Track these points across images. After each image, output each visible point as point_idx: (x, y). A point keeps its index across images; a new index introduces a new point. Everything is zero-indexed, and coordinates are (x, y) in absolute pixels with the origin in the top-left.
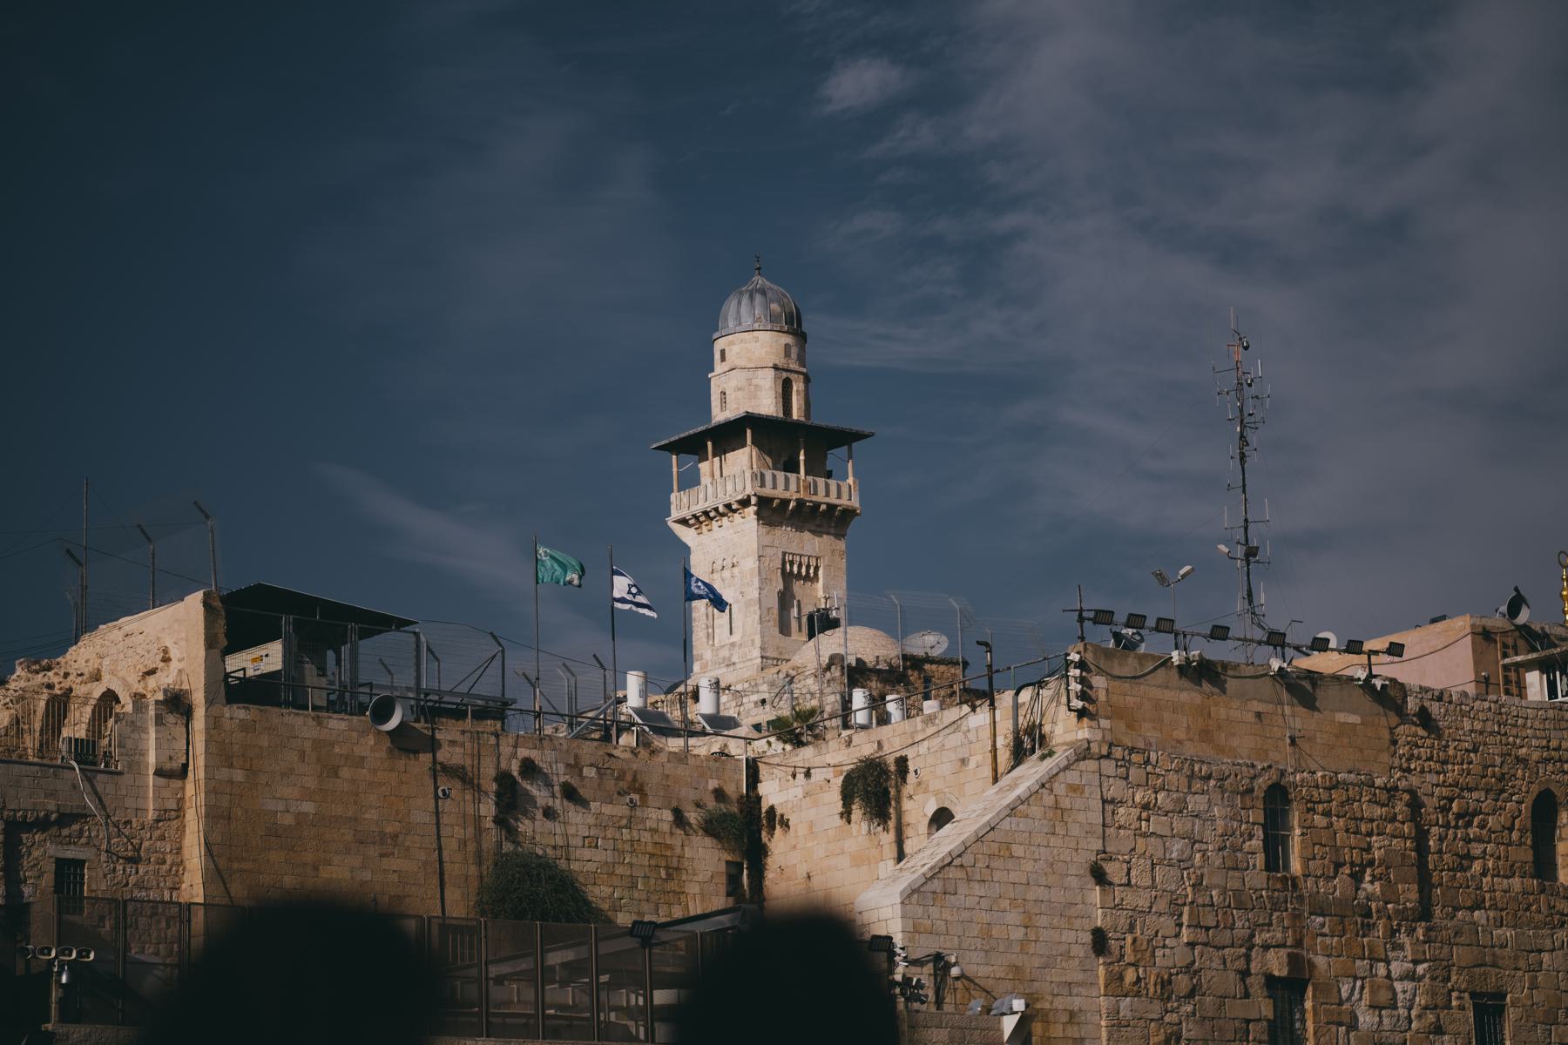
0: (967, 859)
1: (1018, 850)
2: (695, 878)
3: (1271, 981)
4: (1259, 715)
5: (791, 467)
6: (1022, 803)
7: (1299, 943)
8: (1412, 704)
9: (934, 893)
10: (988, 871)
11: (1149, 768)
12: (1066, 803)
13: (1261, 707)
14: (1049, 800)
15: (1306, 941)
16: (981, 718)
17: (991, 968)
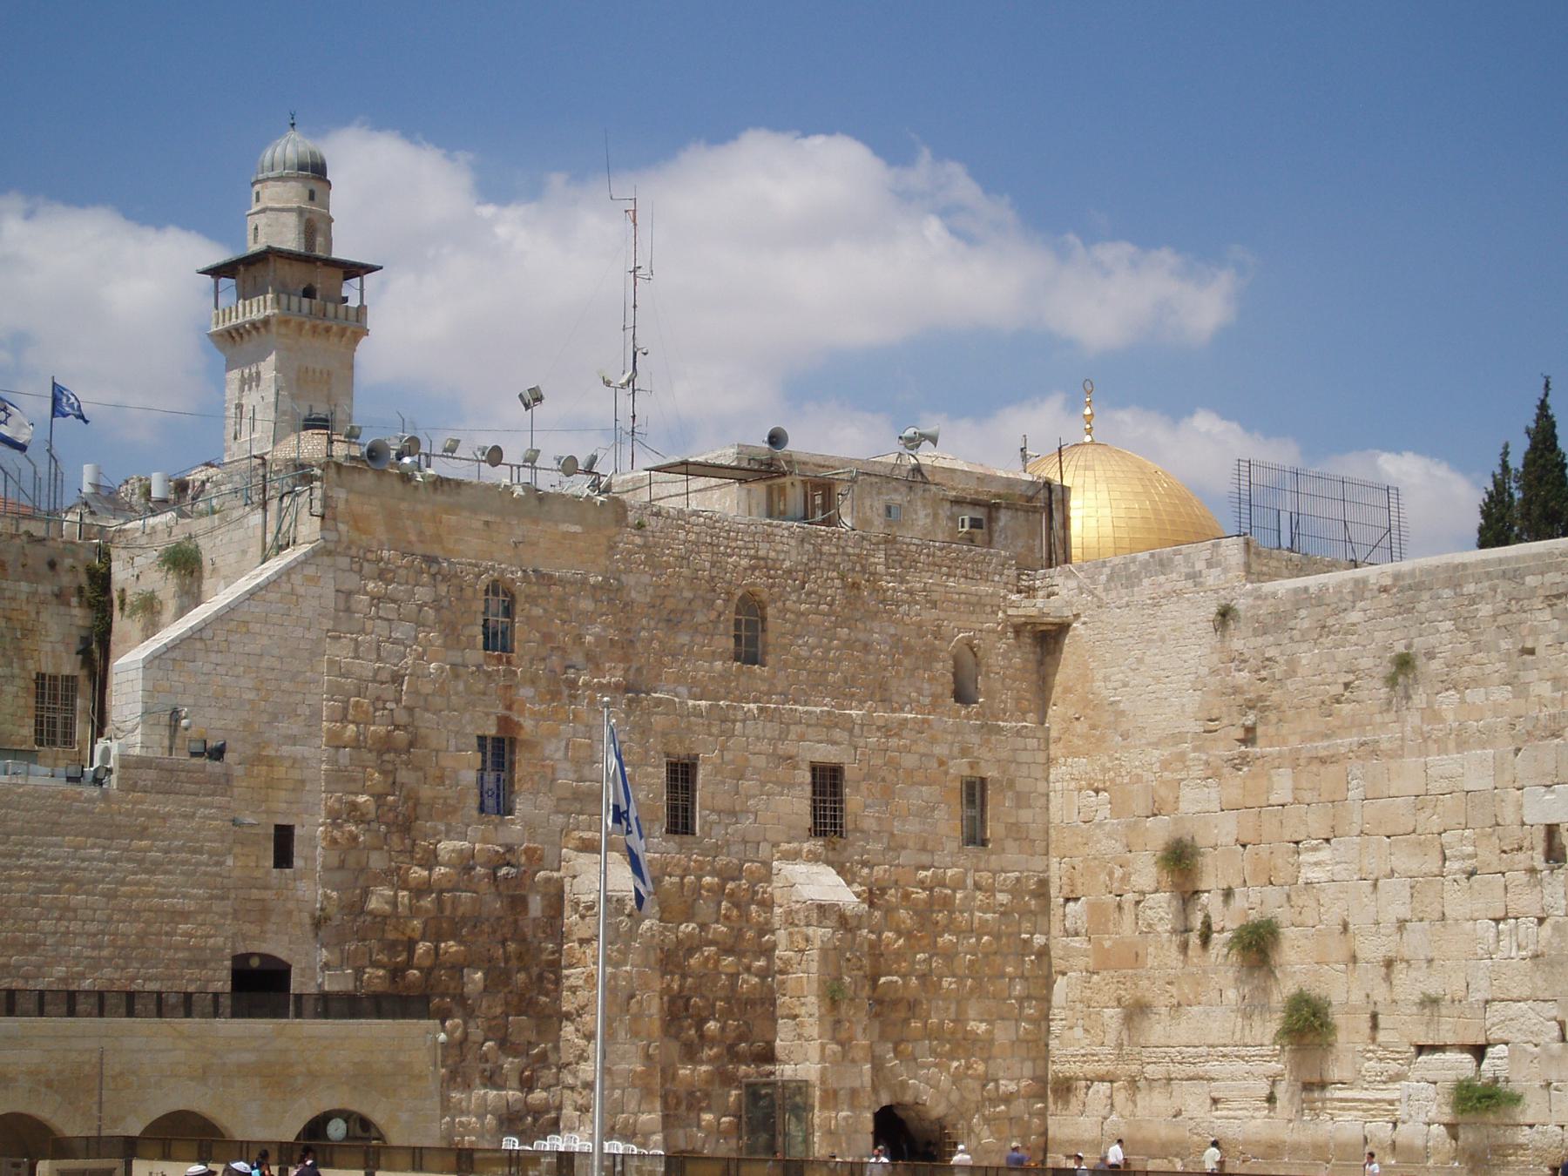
0: (208, 634)
1: (256, 627)
2: (49, 639)
3: (482, 739)
4: (487, 523)
5: (309, 293)
6: (261, 589)
7: (509, 708)
8: (632, 517)
9: (174, 660)
10: (225, 644)
11: (381, 564)
12: (301, 590)
13: (488, 518)
14: (286, 587)
15: (515, 707)
16: (256, 518)
17: (223, 722)
